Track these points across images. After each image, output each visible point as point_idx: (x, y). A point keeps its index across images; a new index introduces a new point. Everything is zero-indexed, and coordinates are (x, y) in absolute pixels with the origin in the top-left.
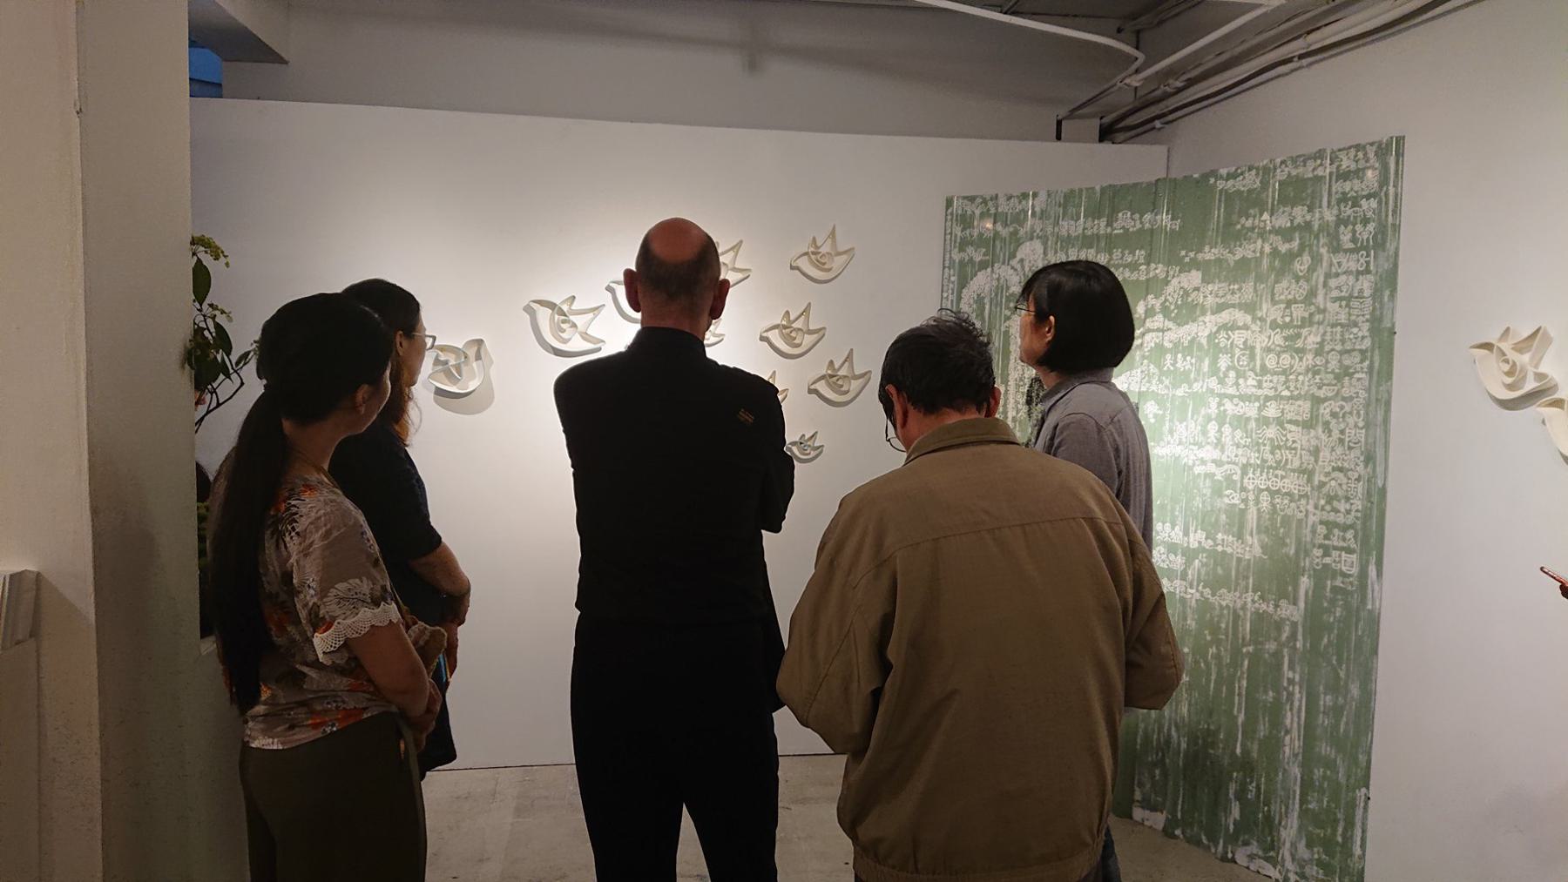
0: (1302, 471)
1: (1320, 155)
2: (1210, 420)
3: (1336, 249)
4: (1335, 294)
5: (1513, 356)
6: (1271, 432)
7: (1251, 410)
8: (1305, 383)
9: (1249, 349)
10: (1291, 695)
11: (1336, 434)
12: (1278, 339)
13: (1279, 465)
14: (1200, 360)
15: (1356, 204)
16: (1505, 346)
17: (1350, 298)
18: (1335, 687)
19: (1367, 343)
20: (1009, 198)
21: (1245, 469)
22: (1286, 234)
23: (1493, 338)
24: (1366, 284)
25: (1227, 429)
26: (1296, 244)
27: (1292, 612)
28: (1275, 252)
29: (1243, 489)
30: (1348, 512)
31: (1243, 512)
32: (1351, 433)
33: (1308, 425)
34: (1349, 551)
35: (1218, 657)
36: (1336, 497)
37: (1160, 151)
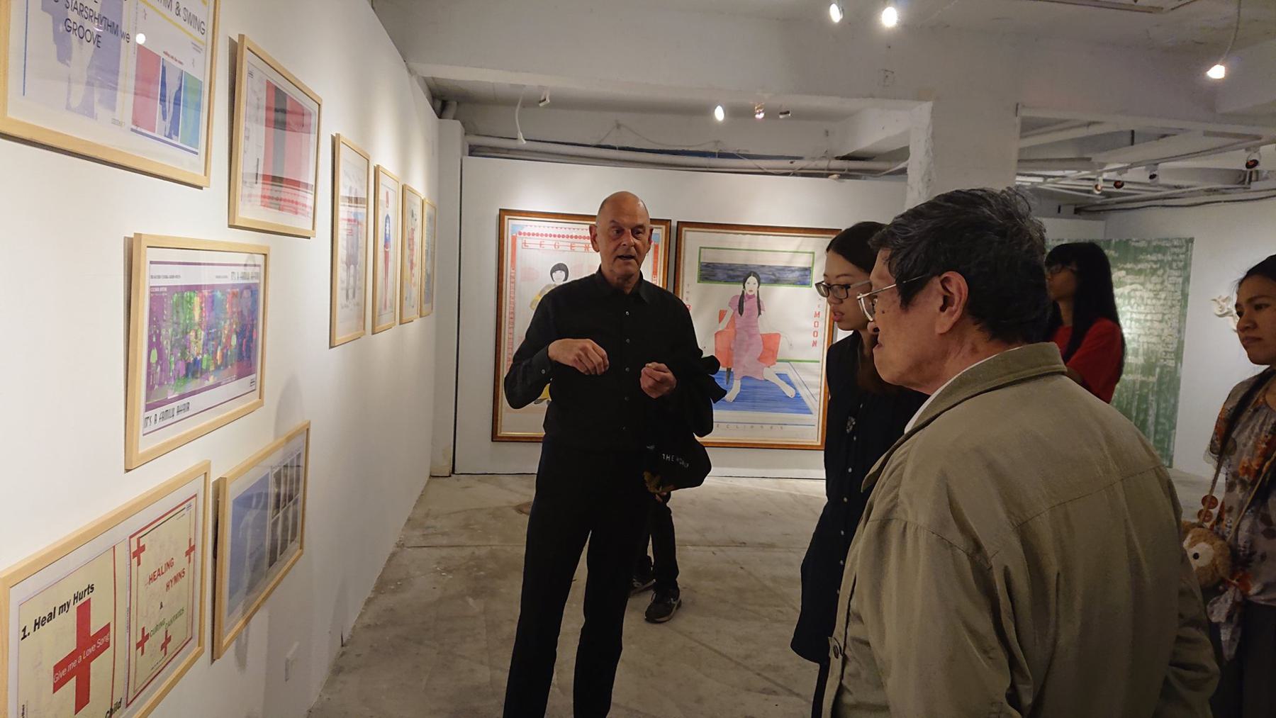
0: (1157, 336)
1: (1167, 239)
2: (1127, 319)
3: (1171, 268)
4: (1171, 282)
5: (1222, 303)
6: (1148, 324)
7: (1142, 317)
8: (1160, 309)
9: (1142, 298)
10: (1151, 405)
11: (1169, 325)
12: (1152, 295)
13: (1151, 334)
14: (1125, 300)
15: (1178, 255)
16: (1220, 300)
17: (1175, 284)
18: (1166, 401)
19: (1180, 297)
20: (1053, 240)
21: (1139, 335)
22: (1156, 262)
23: (1216, 298)
24: (1180, 280)
25: (1133, 323)
26: (1158, 266)
27: (1153, 379)
28: (1151, 268)
29: (1138, 342)
30: (1172, 348)
31: (1138, 349)
32: (1174, 325)
33: (1161, 321)
34: (1172, 359)
35: (1127, 396)
36: (1169, 344)
37: (1100, 224)
